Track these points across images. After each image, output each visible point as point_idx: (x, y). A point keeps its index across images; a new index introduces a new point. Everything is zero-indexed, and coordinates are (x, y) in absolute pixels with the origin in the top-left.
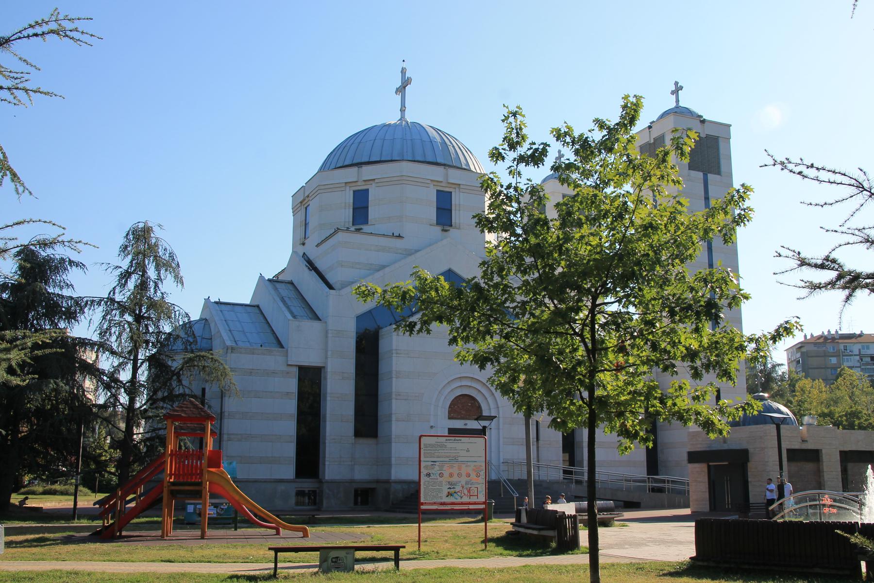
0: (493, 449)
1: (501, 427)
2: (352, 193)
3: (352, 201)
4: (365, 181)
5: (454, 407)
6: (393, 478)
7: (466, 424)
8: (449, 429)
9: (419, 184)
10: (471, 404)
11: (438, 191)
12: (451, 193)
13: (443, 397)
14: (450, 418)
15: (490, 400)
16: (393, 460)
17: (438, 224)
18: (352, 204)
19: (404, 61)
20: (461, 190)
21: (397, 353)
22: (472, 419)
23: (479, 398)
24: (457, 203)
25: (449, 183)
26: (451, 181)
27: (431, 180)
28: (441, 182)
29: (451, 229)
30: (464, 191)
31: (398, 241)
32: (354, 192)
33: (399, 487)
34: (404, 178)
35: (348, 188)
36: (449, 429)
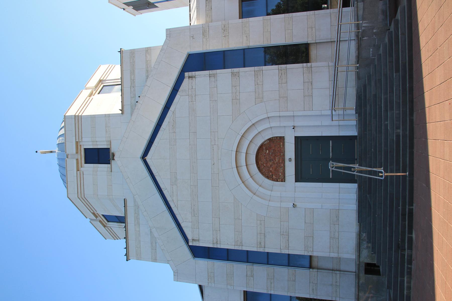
0: (317, 123)
1: (291, 114)
2: (109, 223)
3: (116, 224)
4: (97, 217)
5: (271, 171)
6: (354, 257)
7: (290, 160)
8: (296, 182)
9: (82, 182)
10: (266, 149)
11: (86, 162)
12: (85, 149)
13: (261, 189)
14: (283, 180)
15: (260, 128)
16: (332, 255)
17: (109, 163)
18: (118, 224)
19: (37, 152)
20: (80, 140)
21: (217, 243)
22: (284, 148)
23: (259, 142)
24: (91, 143)
25: (77, 153)
26: (75, 152)
27: (78, 170)
28: (77, 160)
29: (112, 150)
30: (80, 137)
31: (128, 204)
32: (108, 221)
33: (365, 253)
34: (80, 196)
35: (108, 225)
36: (297, 181)
